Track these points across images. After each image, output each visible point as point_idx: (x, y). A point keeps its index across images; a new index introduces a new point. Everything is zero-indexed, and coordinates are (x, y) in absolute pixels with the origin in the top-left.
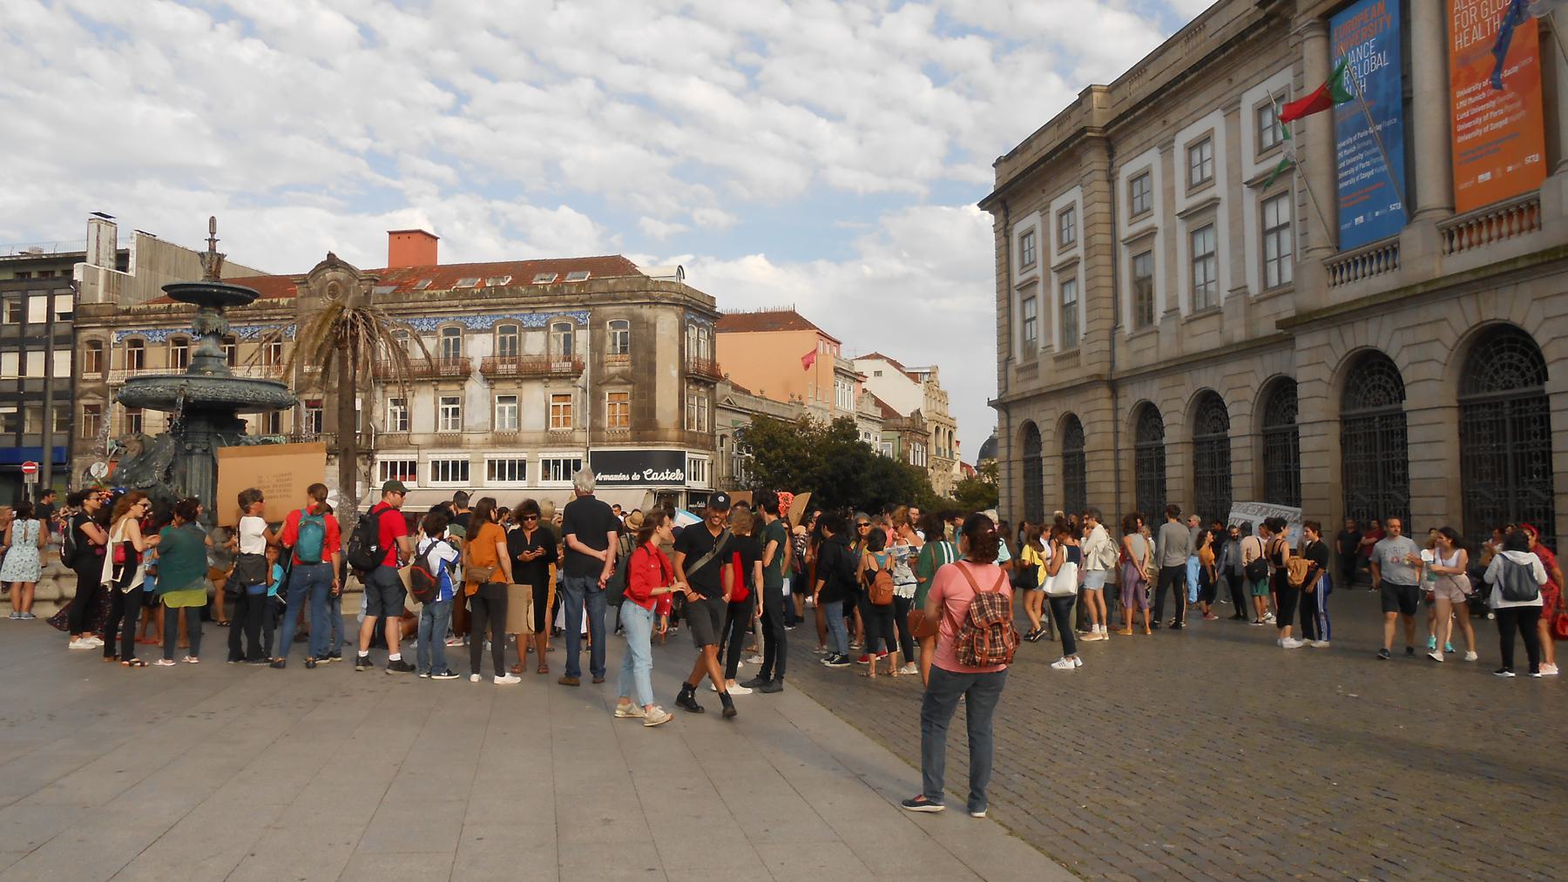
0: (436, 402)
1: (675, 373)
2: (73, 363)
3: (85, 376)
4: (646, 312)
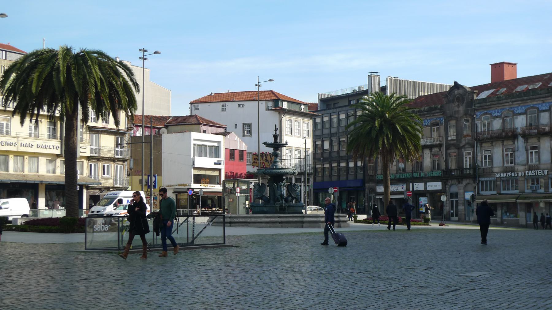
0: (503, 151)
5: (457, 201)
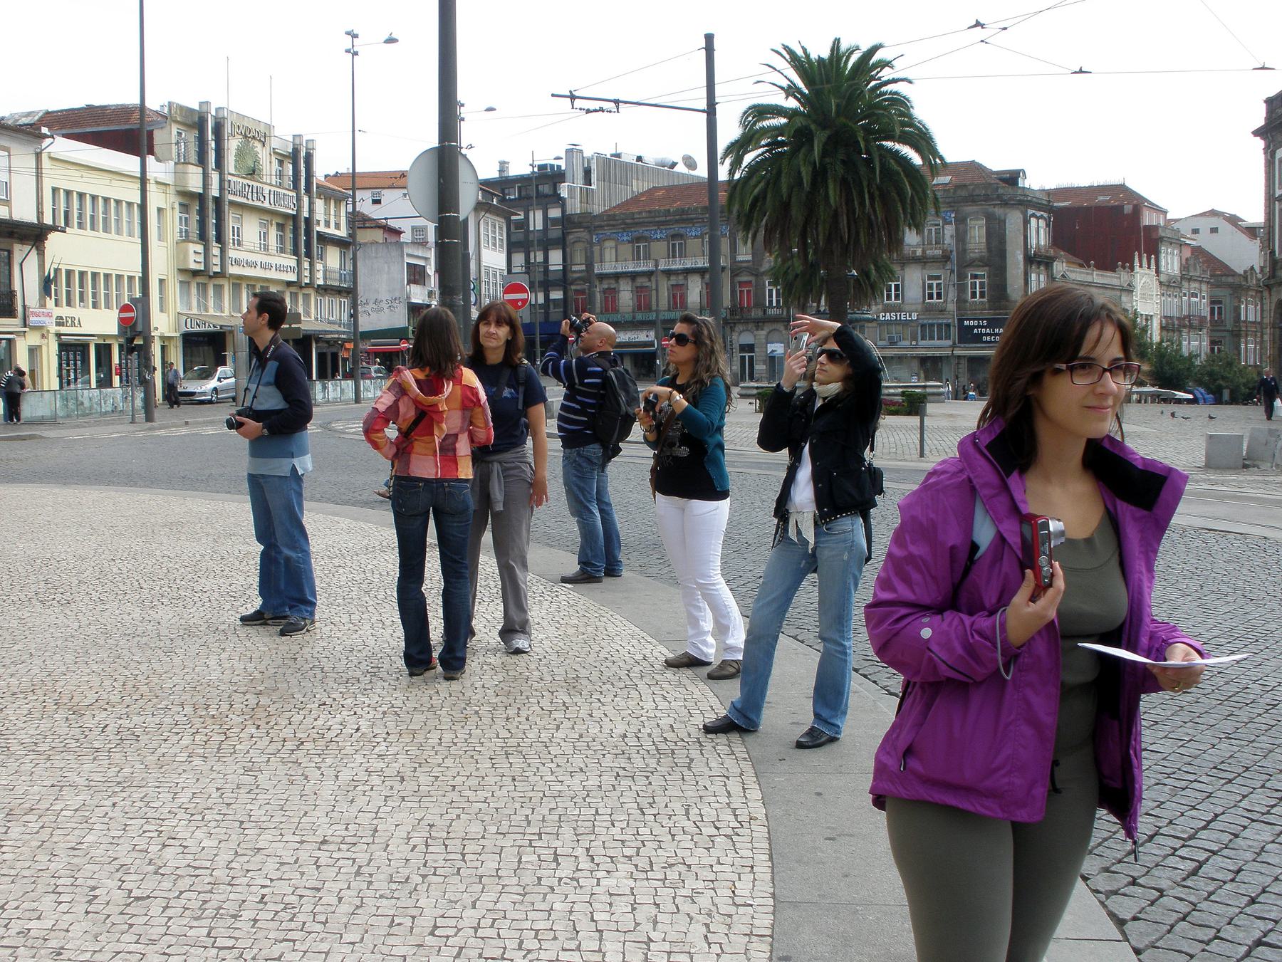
1: (1021, 257)
2: (564, 259)
3: (574, 268)
4: (998, 211)
5: (751, 358)
